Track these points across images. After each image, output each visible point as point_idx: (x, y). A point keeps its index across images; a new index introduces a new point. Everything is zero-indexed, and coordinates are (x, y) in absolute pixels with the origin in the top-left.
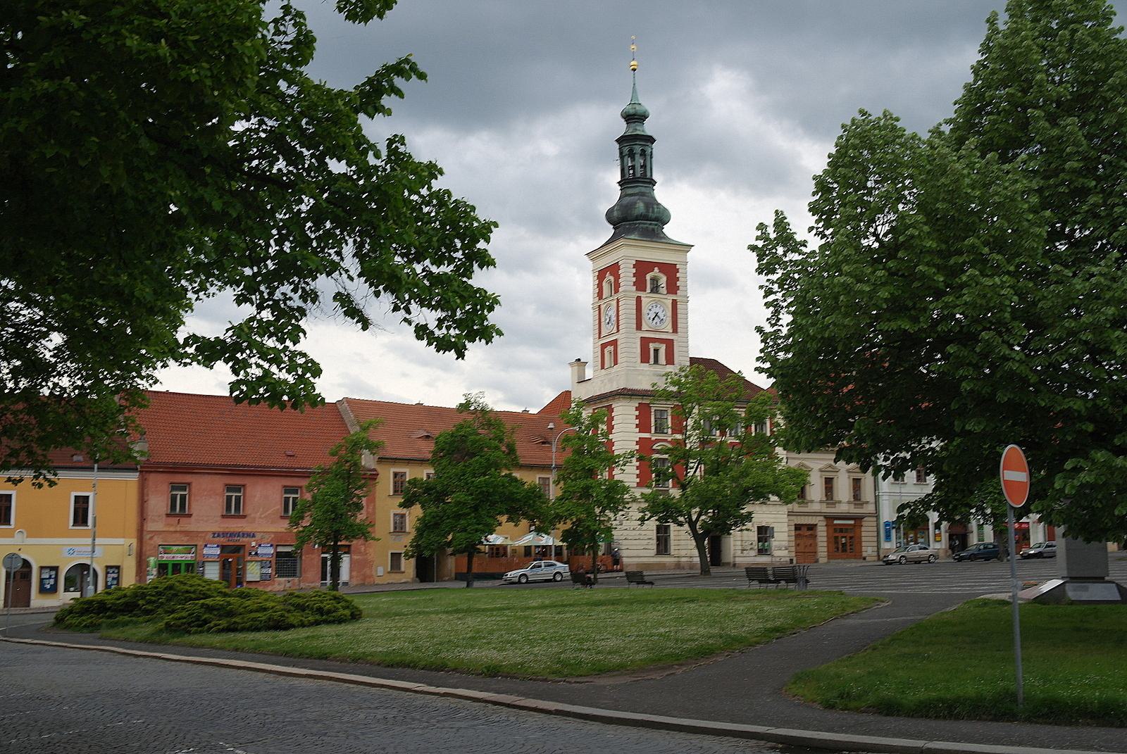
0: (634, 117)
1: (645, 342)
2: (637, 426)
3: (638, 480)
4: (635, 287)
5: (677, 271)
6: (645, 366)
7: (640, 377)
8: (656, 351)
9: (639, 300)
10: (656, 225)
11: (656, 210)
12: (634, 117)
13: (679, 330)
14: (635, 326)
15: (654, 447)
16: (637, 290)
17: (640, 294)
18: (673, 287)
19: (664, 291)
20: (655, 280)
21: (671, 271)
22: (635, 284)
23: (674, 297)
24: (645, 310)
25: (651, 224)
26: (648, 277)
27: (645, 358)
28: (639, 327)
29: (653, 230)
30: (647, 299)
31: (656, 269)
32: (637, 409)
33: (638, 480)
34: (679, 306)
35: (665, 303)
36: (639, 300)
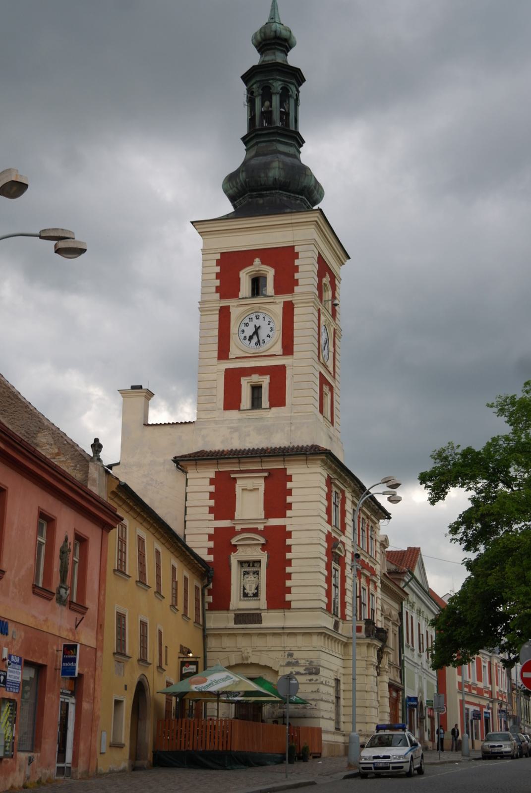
0: (273, 41)
1: (233, 378)
4: (218, 295)
5: (296, 255)
6: (233, 414)
9: (224, 313)
12: (273, 41)
13: (295, 348)
14: (216, 354)
16: (222, 297)
17: (225, 303)
18: (286, 282)
19: (270, 288)
21: (283, 259)
22: (218, 289)
23: (287, 298)
24: (234, 329)
27: (232, 401)
28: (223, 353)
31: (257, 261)
34: (296, 311)
35: (268, 310)
36: (224, 313)
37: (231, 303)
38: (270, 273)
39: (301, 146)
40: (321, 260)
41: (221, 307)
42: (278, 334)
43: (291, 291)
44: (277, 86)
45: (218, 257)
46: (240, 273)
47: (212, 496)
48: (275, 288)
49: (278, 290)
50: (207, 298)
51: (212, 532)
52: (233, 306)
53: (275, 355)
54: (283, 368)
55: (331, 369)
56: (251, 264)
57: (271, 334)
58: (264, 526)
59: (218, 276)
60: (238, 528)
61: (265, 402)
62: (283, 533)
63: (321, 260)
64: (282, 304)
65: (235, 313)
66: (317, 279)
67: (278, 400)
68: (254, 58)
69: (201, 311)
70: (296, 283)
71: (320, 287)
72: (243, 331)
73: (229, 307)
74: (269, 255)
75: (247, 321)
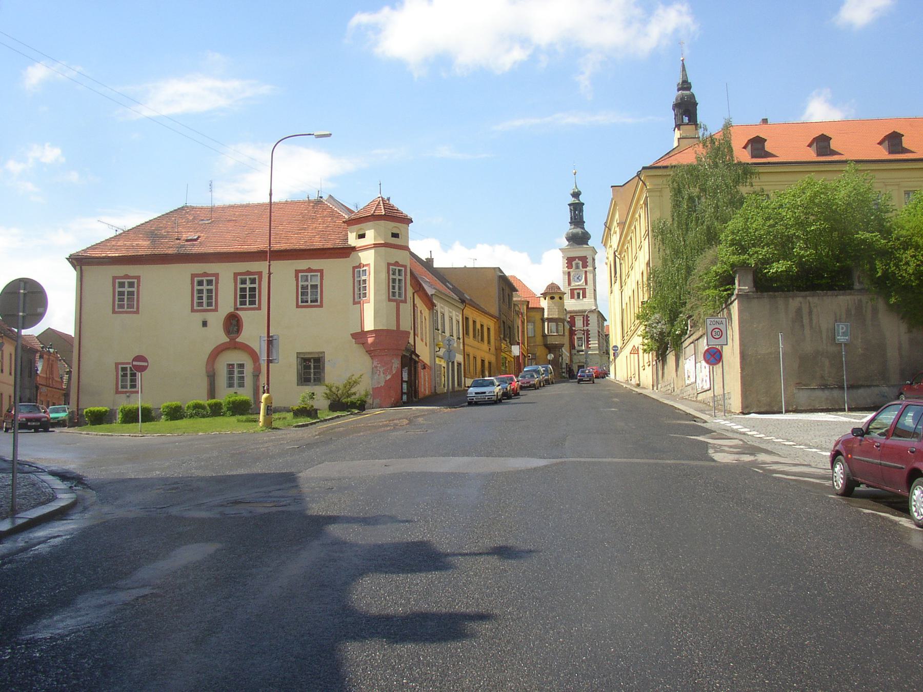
1: (572, 291)
6: (573, 301)
8: (579, 294)
9: (569, 273)
20: (577, 264)
21: (584, 260)
26: (574, 263)
27: (572, 297)
28: (569, 284)
36: (569, 273)
62: (588, 331)
67: (584, 296)
68: (572, 200)
74: (581, 258)
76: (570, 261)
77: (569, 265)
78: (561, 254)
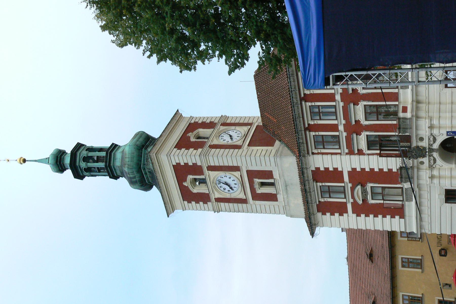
1: (257, 197)
2: (341, 214)
3: (397, 217)
5: (178, 164)
7: (292, 205)
10: (144, 169)
11: (131, 176)
13: (235, 165)
14: (244, 205)
15: (360, 202)
16: (210, 201)
18: (196, 169)
21: (181, 171)
22: (205, 202)
24: (228, 196)
25: (146, 174)
27: (272, 198)
28: (244, 201)
29: (150, 172)
30: (215, 192)
32: (324, 214)
33: (397, 217)
34: (212, 164)
36: (219, 200)
37: (213, 197)
38: (190, 177)
39: (116, 145)
40: (179, 146)
41: (216, 201)
42: (228, 174)
43: (200, 167)
44: (83, 165)
45: (186, 202)
46: (194, 192)
47: (332, 214)
48: (200, 175)
49: (202, 173)
50: (211, 208)
51: (355, 215)
52: (214, 196)
53: (241, 176)
54: (247, 171)
55: (246, 128)
56: (187, 187)
57: (228, 177)
58: (350, 183)
59: (197, 202)
60: (351, 200)
61: (271, 181)
63: (179, 146)
64: (210, 172)
65: (217, 195)
66: (191, 150)
67: (269, 174)
69: (220, 211)
70: (195, 165)
71: (196, 146)
72: (229, 191)
73: (215, 199)
75: (222, 189)
76: (189, 197)
77: (203, 198)
78: (178, 213)
